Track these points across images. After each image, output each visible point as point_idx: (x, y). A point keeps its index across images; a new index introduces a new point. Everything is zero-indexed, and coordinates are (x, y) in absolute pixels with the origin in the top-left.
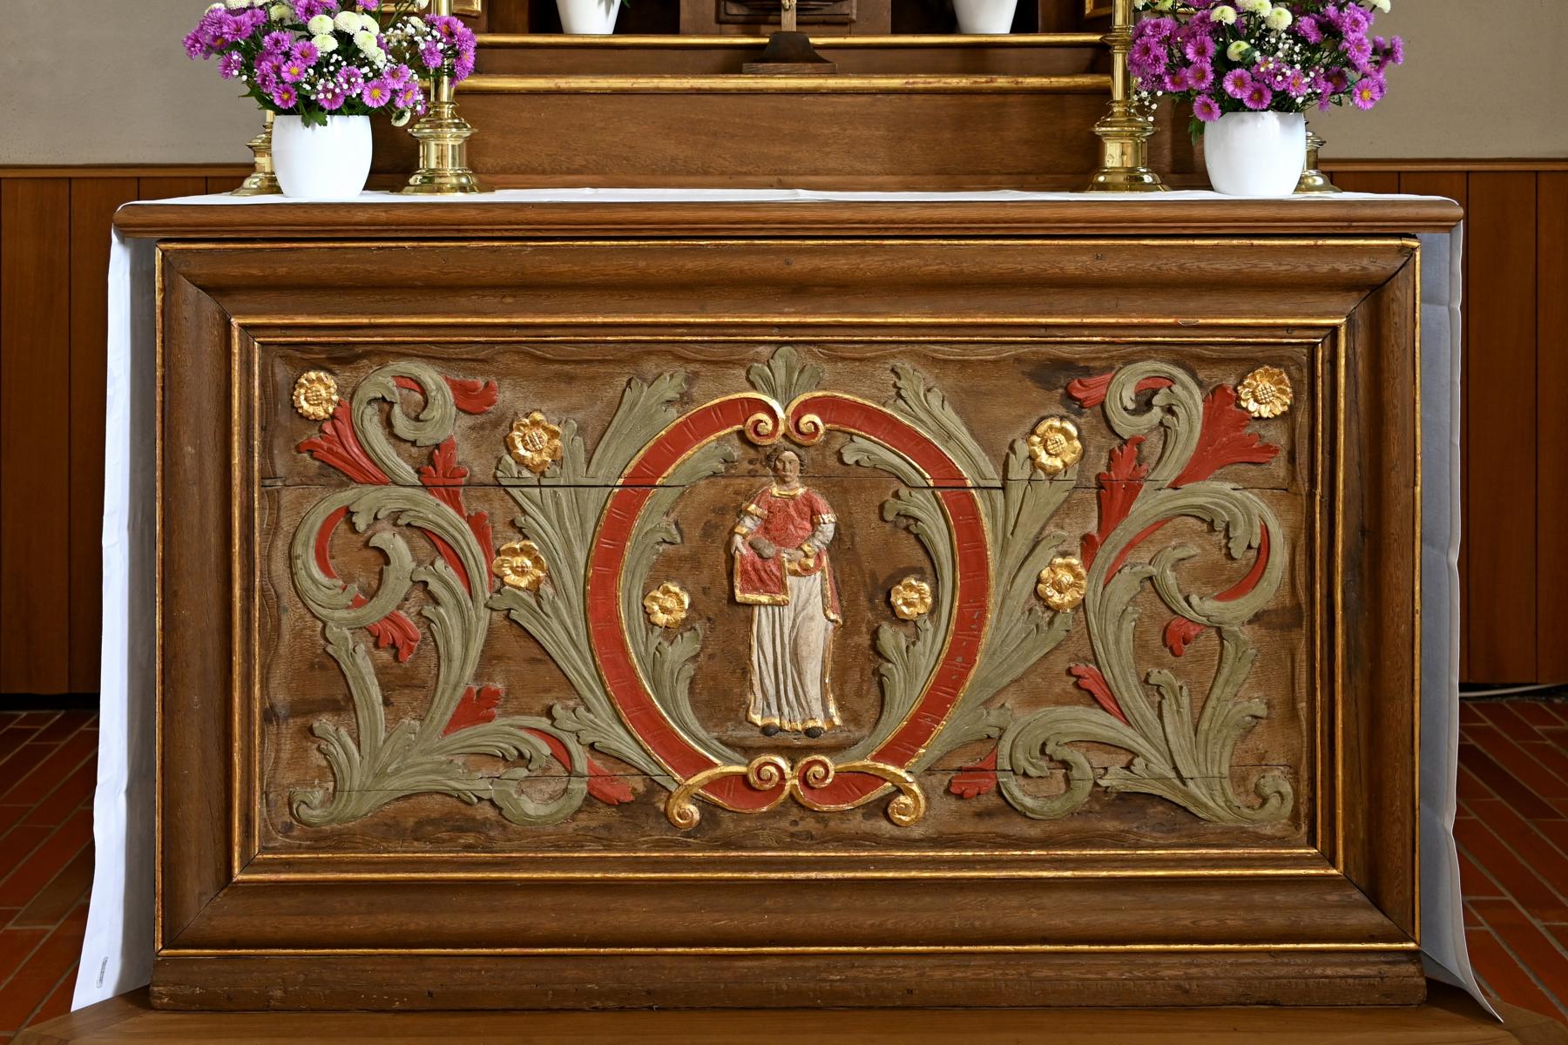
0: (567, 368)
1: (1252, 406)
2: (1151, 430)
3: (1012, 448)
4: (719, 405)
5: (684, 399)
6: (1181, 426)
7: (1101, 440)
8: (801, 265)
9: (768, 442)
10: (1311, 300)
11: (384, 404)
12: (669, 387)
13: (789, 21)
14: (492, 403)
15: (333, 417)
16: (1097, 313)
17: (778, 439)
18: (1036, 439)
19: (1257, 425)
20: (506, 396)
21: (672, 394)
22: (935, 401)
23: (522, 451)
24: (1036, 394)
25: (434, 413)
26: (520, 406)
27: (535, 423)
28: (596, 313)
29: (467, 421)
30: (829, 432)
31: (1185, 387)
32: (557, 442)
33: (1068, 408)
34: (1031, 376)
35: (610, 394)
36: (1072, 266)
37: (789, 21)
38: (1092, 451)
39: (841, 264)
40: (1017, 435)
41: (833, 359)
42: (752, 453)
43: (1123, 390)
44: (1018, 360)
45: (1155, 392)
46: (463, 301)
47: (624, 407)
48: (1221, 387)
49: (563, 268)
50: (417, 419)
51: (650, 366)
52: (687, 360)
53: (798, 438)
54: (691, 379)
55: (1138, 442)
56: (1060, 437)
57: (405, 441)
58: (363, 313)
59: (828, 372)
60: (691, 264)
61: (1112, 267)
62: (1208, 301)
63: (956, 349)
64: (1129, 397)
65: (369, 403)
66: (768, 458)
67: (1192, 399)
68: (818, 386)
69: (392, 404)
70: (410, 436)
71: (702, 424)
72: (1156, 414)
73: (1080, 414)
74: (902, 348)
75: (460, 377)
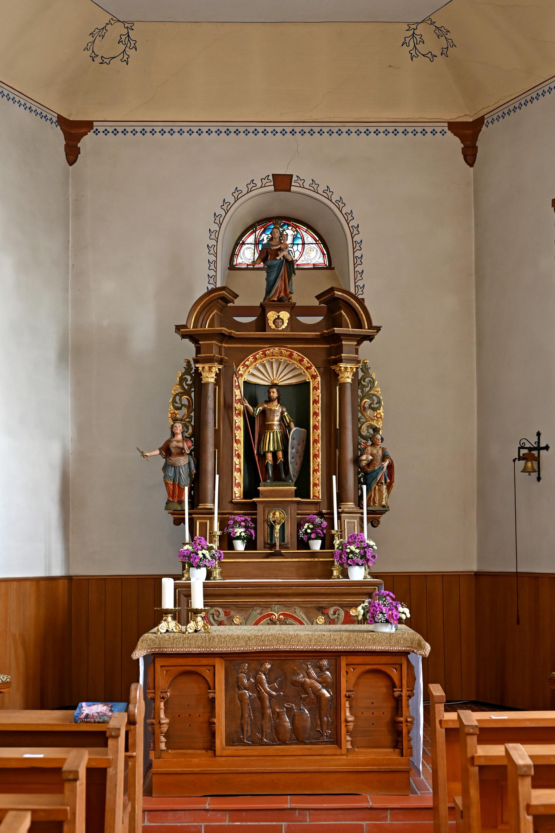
0: (242, 608)
1: (352, 614)
2: (336, 618)
3: (313, 621)
4: (266, 614)
5: (261, 614)
6: (340, 617)
7: (328, 619)
8: (279, 591)
9: (274, 620)
10: (361, 596)
11: (213, 614)
12: (258, 611)
13: (278, 548)
14: (230, 614)
15: (205, 617)
16: (326, 599)
17: (276, 620)
18: (317, 619)
19: (353, 617)
20: (232, 613)
21: (259, 613)
22: (301, 613)
23: (235, 622)
24: (317, 612)
25: (221, 616)
26: (234, 615)
27: (237, 617)
28: (247, 599)
29: (226, 617)
30: (284, 618)
31: (341, 611)
32: (241, 620)
33: (323, 614)
34: (316, 609)
35: (249, 613)
36: (322, 591)
37: (278, 548)
38: (326, 621)
39: (285, 591)
40: (314, 619)
41: (285, 607)
42: (272, 622)
43: (331, 611)
44: (314, 607)
45: (336, 612)
46: (226, 598)
47: (251, 615)
48: (347, 611)
49: (242, 592)
50: (218, 617)
51: (255, 608)
52: (261, 607)
53: (279, 620)
54: (262, 610)
55: (334, 620)
56: (321, 619)
57: (216, 620)
58: (210, 600)
59: (284, 609)
60: (262, 591)
61: (329, 591)
62: (344, 597)
63: (304, 605)
64: (332, 612)
65: (211, 614)
66: (274, 623)
67: (342, 613)
68: (282, 611)
69: (214, 614)
70: (217, 619)
71: (264, 617)
72: (336, 615)
73: (324, 615)
74: (296, 605)
75: (225, 610)
